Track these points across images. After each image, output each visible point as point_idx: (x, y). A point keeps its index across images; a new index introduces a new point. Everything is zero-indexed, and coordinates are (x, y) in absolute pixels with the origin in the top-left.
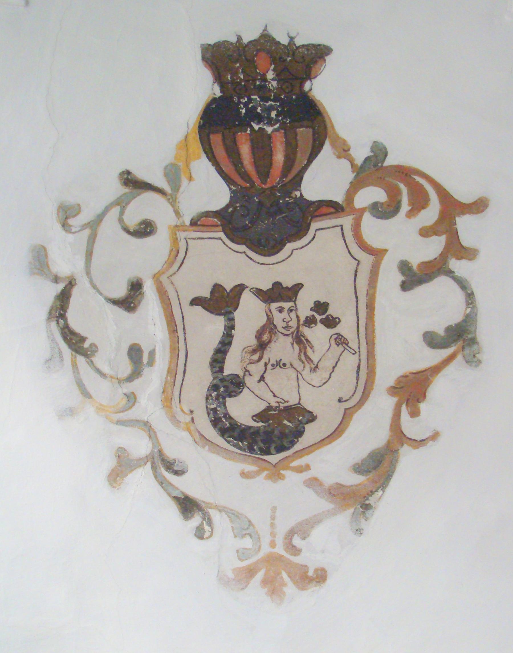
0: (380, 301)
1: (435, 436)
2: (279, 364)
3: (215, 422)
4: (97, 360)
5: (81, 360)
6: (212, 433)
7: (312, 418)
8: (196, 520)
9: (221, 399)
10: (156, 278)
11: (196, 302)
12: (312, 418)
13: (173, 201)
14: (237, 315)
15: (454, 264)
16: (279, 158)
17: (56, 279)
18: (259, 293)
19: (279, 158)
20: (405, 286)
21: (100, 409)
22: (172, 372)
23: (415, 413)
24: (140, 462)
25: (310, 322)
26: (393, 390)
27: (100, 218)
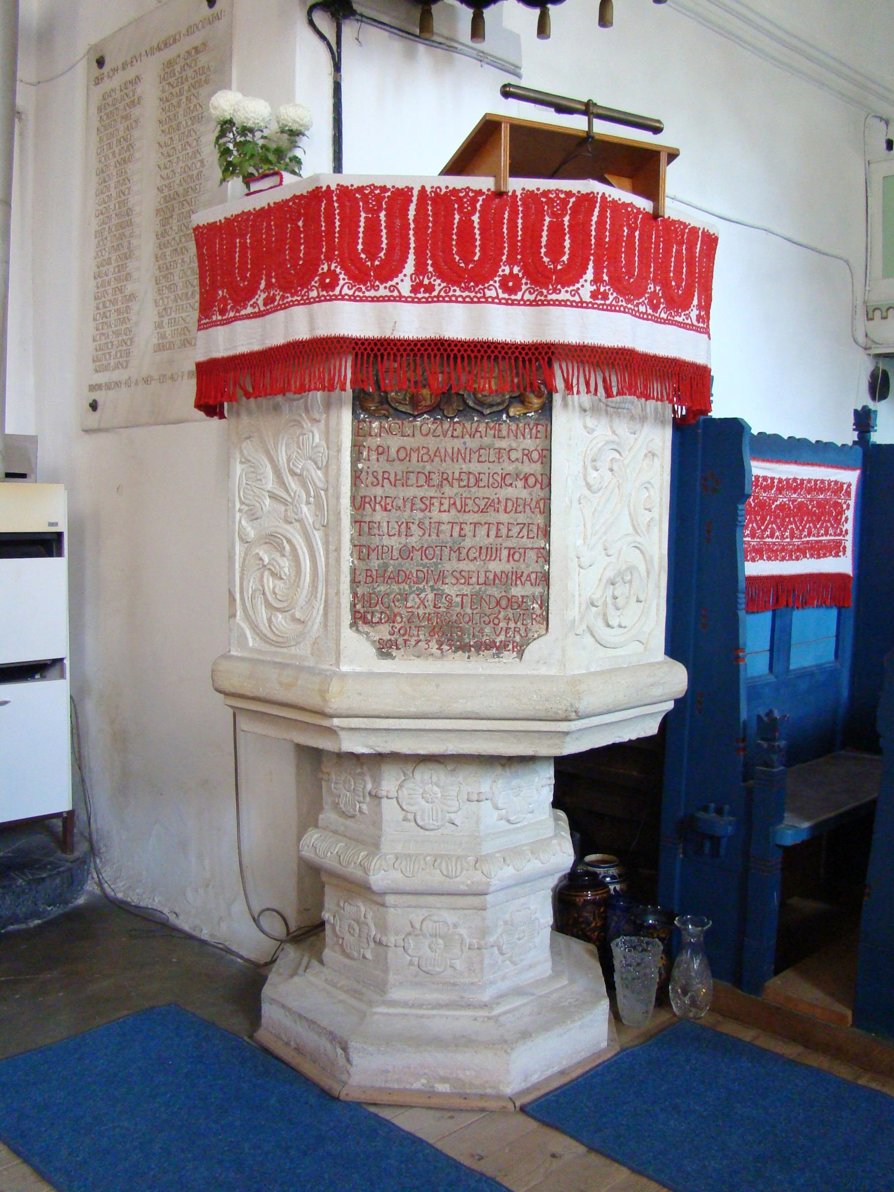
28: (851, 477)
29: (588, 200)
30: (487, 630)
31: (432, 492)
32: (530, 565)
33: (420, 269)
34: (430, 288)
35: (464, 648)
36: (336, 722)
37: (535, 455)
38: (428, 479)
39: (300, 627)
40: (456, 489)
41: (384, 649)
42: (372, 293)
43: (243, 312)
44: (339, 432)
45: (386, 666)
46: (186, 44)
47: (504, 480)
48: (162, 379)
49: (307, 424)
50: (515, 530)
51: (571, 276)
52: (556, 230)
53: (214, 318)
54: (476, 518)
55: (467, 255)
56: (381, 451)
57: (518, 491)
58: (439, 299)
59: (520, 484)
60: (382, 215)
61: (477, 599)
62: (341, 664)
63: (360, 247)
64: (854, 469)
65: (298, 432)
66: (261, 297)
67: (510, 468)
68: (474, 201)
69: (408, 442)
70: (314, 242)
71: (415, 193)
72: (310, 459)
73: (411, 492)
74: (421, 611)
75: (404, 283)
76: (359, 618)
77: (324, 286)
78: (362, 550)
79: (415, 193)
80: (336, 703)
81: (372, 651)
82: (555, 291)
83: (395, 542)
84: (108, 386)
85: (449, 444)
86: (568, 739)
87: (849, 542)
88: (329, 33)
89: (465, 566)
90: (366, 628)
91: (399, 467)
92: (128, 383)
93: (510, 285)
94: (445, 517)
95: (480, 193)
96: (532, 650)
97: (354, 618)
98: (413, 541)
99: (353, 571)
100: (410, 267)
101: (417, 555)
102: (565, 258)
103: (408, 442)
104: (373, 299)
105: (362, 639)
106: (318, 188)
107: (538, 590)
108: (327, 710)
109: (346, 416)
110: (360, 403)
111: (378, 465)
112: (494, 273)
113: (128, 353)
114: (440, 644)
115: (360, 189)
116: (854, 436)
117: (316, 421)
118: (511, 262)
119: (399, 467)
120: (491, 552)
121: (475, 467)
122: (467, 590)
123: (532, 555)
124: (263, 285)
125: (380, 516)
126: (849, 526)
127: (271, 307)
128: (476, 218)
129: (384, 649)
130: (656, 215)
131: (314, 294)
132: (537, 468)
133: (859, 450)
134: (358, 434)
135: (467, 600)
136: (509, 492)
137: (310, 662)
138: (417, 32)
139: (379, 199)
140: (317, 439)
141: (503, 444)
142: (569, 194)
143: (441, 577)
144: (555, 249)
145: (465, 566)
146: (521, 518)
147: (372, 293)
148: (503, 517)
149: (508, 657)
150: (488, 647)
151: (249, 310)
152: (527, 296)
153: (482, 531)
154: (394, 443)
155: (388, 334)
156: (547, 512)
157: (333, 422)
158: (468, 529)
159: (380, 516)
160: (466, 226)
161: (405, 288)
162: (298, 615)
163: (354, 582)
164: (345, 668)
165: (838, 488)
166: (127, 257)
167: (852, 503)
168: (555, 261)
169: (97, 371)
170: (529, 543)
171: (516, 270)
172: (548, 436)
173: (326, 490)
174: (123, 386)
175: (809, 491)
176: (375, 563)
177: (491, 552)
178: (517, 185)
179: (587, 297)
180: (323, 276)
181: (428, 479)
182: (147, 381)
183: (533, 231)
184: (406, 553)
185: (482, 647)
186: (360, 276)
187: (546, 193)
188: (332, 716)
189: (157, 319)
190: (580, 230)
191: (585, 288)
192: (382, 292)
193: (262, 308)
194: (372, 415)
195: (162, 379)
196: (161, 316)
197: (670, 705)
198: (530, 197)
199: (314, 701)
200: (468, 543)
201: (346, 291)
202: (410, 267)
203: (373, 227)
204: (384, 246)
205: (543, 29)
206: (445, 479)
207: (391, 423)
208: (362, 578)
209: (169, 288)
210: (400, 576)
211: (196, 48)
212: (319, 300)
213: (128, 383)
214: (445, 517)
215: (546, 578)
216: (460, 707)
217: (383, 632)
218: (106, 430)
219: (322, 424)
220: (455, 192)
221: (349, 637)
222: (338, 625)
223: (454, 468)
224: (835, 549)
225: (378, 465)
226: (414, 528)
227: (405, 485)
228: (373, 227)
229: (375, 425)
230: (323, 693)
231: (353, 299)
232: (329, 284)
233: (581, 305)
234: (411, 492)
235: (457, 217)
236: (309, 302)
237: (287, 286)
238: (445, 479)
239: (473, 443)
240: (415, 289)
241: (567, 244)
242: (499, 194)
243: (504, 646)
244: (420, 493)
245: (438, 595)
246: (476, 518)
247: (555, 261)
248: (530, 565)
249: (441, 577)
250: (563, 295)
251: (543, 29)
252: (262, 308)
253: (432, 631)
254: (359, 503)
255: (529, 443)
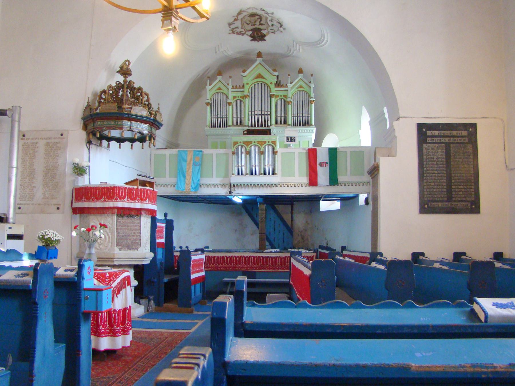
0: (241, 26)
1: (232, 17)
2: (253, 20)
3: (261, 16)
4: (276, 21)
5: (278, 22)
6: (261, 15)
7: (248, 17)
8: (262, 9)
9: (260, 17)
10: (270, 26)
11: (264, 24)
12: (248, 17)
13: (268, 32)
14: (259, 23)
15: (232, 29)
16: (255, 34)
17: (282, 28)
18: (256, 25)
19: (255, 34)
20: (238, 27)
21: (276, 18)
22: (267, 20)
23: (235, 18)
24: (270, 14)
25: (250, 23)
26: (238, 19)
27: (277, 31)
28: (164, 225)
29: (147, 190)
30: (133, 247)
31: (126, 228)
32: (138, 238)
33: (128, 198)
34: (129, 201)
35: (130, 249)
36: (115, 260)
37: (139, 223)
38: (126, 226)
39: (106, 247)
40: (130, 227)
41: (120, 249)
42: (122, 201)
43: (98, 201)
44: (114, 219)
45: (120, 252)
46: (53, 141)
47: (135, 226)
48: (45, 205)
49: (108, 218)
50: (137, 233)
51: (145, 200)
52: (144, 193)
53: (91, 201)
54: (132, 231)
55: (133, 196)
56: (120, 222)
57: (137, 228)
58: (130, 202)
59: (137, 227)
60: (123, 191)
61: (132, 242)
62: (115, 251)
63: (120, 195)
64: (164, 224)
65: (106, 219)
66: (103, 200)
67: (136, 224)
68: (134, 189)
69: (123, 221)
70: (114, 194)
71: (127, 188)
72: (109, 223)
73: (124, 228)
74: (125, 244)
75: (126, 200)
76: (117, 245)
77: (115, 199)
78: (117, 236)
79: (127, 188)
80: (116, 256)
81: (118, 250)
82: (144, 201)
83: (121, 234)
84: (25, 204)
85: (129, 221)
86: (143, 262)
87: (164, 236)
88: (88, 147)
89: (130, 238)
90: (118, 247)
91: (122, 224)
92: (33, 204)
93: (138, 201)
94: (128, 231)
95: (135, 188)
96: (139, 249)
97: (116, 245)
98: (124, 234)
99: (116, 239)
100: (126, 198)
101: (124, 236)
102: (145, 197)
103: (123, 221)
104: (122, 202)
105: (117, 248)
106: (115, 186)
107: (139, 241)
108: (115, 258)
109: (116, 217)
110: (117, 215)
111: (119, 224)
112: (137, 199)
113: (33, 198)
114: (127, 249)
115: (121, 187)
116: (164, 218)
117: (110, 218)
118: (139, 198)
119: (122, 224)
120: (134, 236)
121: (132, 224)
122: (131, 241)
123: (139, 236)
124: (103, 198)
125: (120, 231)
126: (164, 234)
127: (105, 201)
128: (135, 192)
129: (120, 249)
130: (153, 190)
131: (114, 200)
132: (139, 225)
133: (165, 220)
134: (117, 219)
135: (131, 243)
136: (136, 228)
137: (108, 252)
138: (99, 145)
139: (123, 188)
140: (110, 220)
141: (135, 221)
142: (146, 189)
143: (127, 239)
144: (144, 196)
145: (130, 238)
146: (137, 231)
147: (122, 201)
148: (135, 231)
149: (136, 250)
150: (133, 249)
151: (100, 201)
152: (140, 202)
153: (132, 233)
154: (122, 221)
155: (124, 206)
156: (141, 230)
157: (113, 218)
158: (131, 233)
159: (120, 231)
160: (133, 192)
161: (126, 200)
162: (106, 245)
163: (116, 240)
164: (115, 252)
165: (163, 227)
166: (34, 178)
167: (165, 230)
168: (144, 197)
169: (20, 201)
170: (138, 235)
171: (139, 199)
172: (141, 220)
173: (112, 227)
174: (31, 205)
175: (160, 228)
176: (119, 237)
177: (134, 236)
178: (140, 187)
179: (147, 202)
180: (116, 198)
181: (126, 226)
182: (39, 204)
183: (141, 193)
184: (123, 236)
185: (132, 249)
186: (120, 199)
187: (143, 189)
188: (114, 259)
189: (43, 192)
190: (147, 194)
191: (147, 201)
192: (123, 201)
193: (103, 201)
194: (119, 217)
195: (45, 205)
196: (44, 192)
197: (151, 259)
198: (141, 189)
199: (112, 257)
200: (131, 235)
201: (119, 201)
202: (126, 198)
203: (122, 192)
204: (123, 195)
205: (120, 147)
206: (128, 226)
207: (121, 218)
208: (117, 239)
209: (48, 187)
210: (122, 239)
211: (57, 142)
212: (115, 201)
213: (33, 204)
214: (128, 231)
215: (140, 239)
216: (131, 257)
217: (120, 247)
218: (23, 213)
219: (111, 218)
220: (132, 188)
221: (115, 247)
222: (114, 247)
223: (129, 225)
224: (162, 238)
225: (119, 224)
226: (124, 232)
227: (123, 227)
228: (122, 192)
229: (119, 218)
230: (114, 256)
231: (120, 202)
232: (116, 199)
233: (147, 203)
234: (124, 228)
235: (132, 191)
236: (113, 202)
237: (109, 198)
238: (128, 226)
239: (131, 221)
240: (127, 201)
241: (145, 195)
242: (137, 188)
243: (135, 249)
244: (125, 228)
245: (127, 242)
246: (132, 231)
247: (144, 197)
248: (138, 238)
249: (127, 239)
250: (145, 202)
251: (120, 147)
252: (103, 201)
253: (126, 247)
254: (117, 229)
255: (138, 221)
